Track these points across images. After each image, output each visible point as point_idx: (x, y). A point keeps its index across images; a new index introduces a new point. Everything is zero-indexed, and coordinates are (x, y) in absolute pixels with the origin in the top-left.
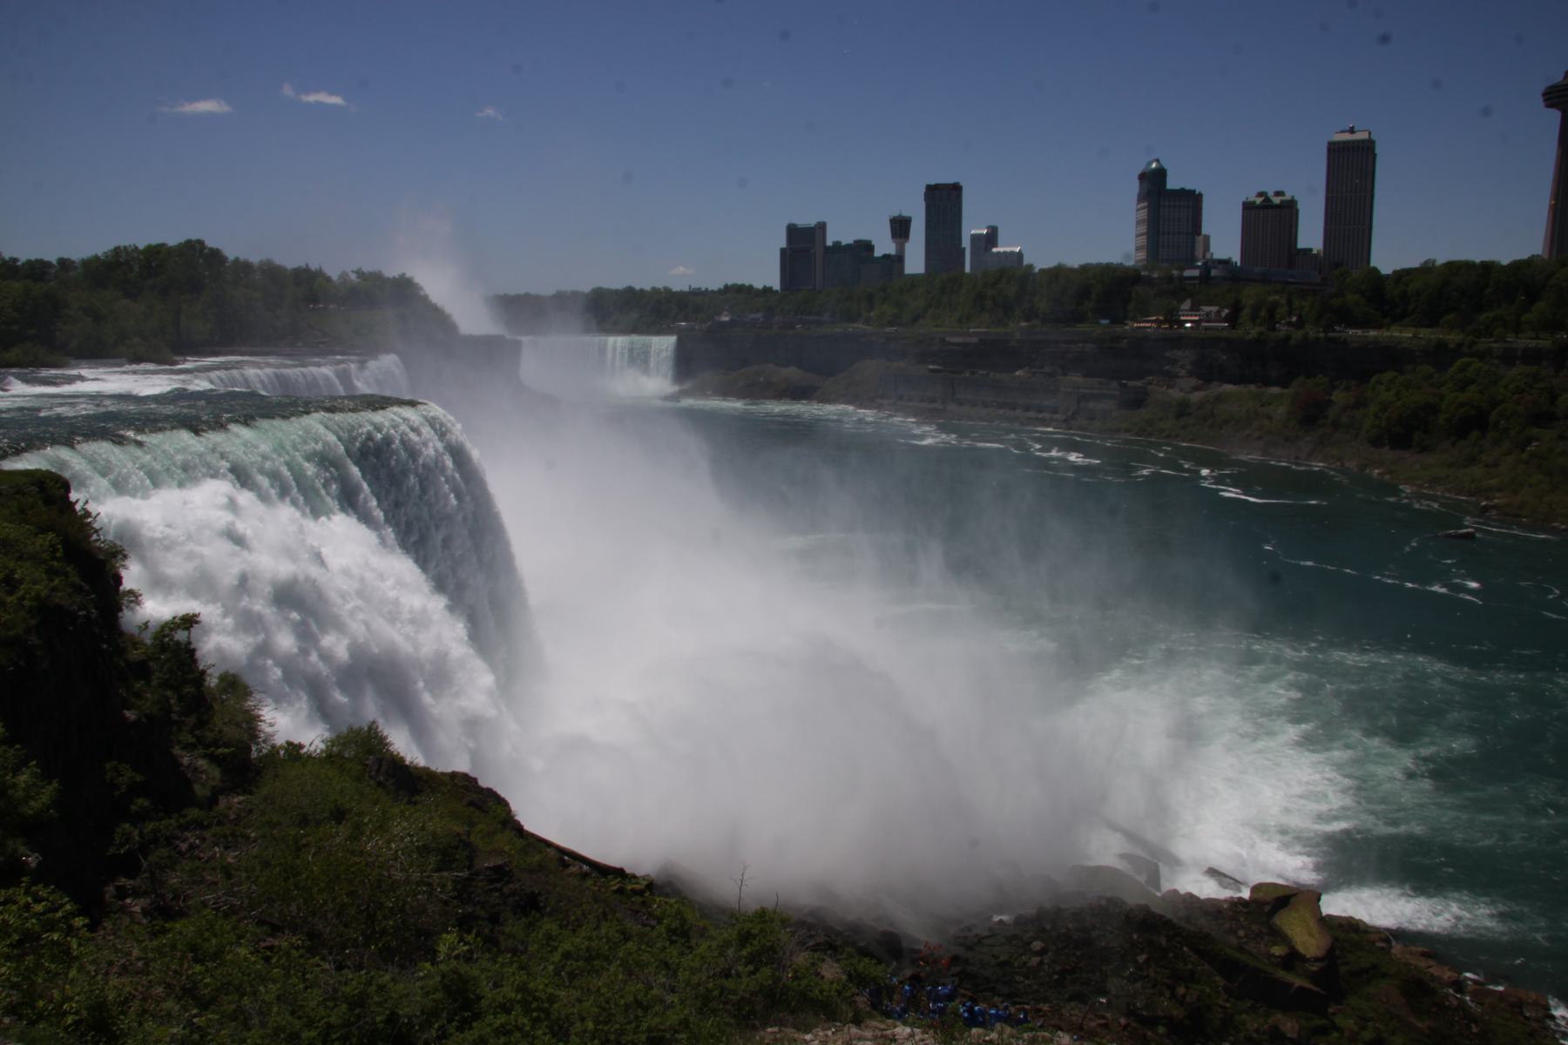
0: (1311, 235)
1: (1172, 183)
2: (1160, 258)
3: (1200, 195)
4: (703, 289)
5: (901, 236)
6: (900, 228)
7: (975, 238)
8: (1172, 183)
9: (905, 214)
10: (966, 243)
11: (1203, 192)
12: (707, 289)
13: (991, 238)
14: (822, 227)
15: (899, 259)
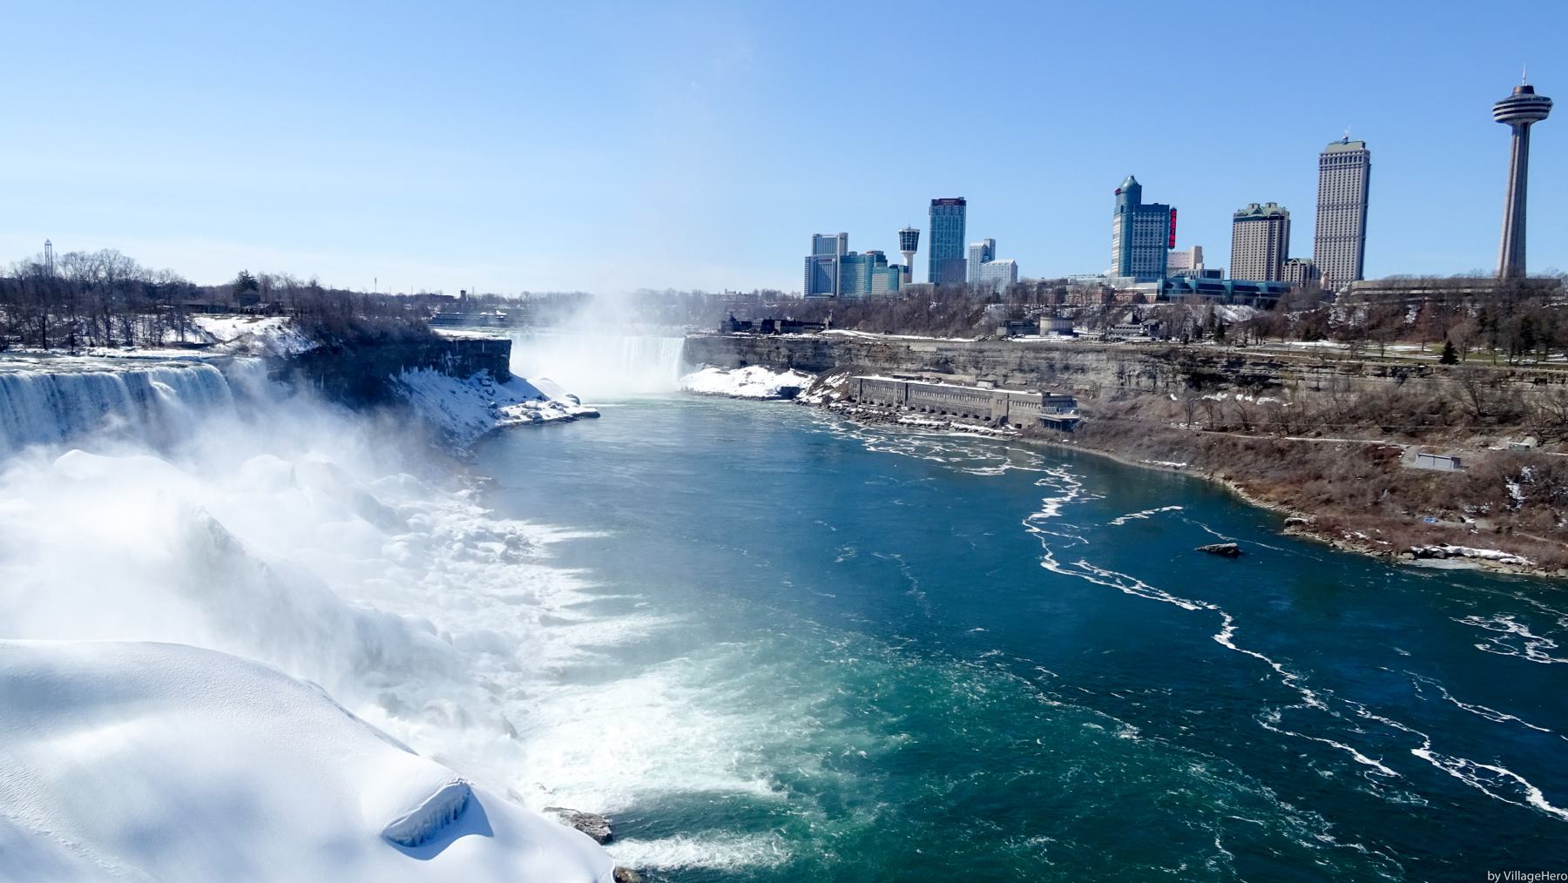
0: (1302, 247)
1: (1147, 199)
2: (1132, 270)
3: (1174, 211)
4: (737, 293)
5: (909, 249)
6: (909, 240)
7: (973, 251)
8: (1147, 199)
9: (914, 227)
10: (966, 255)
11: (1176, 207)
12: (740, 293)
13: (988, 253)
14: (844, 237)
15: (907, 270)
